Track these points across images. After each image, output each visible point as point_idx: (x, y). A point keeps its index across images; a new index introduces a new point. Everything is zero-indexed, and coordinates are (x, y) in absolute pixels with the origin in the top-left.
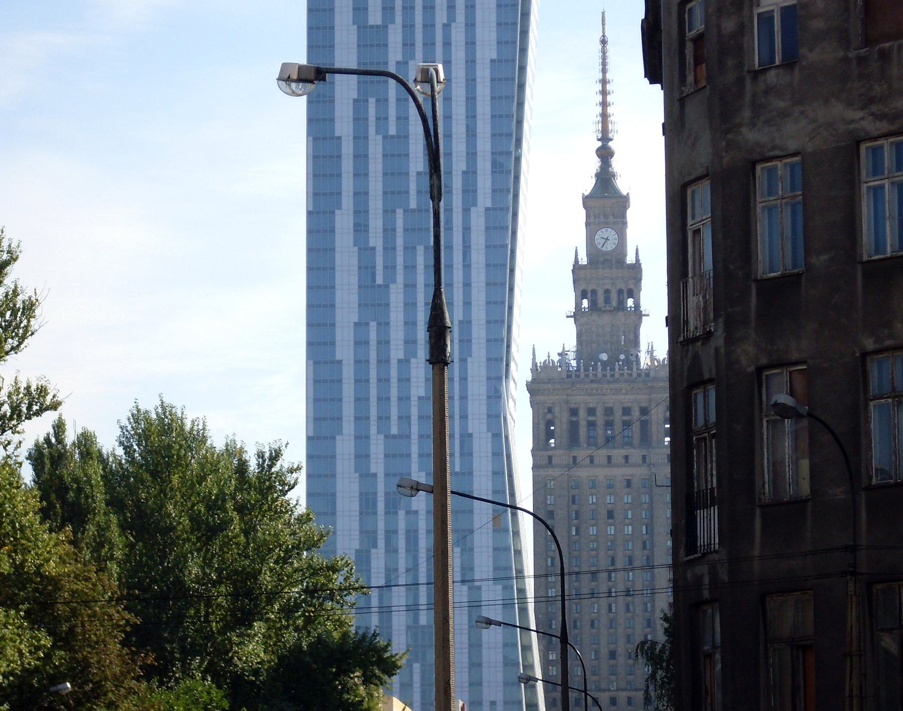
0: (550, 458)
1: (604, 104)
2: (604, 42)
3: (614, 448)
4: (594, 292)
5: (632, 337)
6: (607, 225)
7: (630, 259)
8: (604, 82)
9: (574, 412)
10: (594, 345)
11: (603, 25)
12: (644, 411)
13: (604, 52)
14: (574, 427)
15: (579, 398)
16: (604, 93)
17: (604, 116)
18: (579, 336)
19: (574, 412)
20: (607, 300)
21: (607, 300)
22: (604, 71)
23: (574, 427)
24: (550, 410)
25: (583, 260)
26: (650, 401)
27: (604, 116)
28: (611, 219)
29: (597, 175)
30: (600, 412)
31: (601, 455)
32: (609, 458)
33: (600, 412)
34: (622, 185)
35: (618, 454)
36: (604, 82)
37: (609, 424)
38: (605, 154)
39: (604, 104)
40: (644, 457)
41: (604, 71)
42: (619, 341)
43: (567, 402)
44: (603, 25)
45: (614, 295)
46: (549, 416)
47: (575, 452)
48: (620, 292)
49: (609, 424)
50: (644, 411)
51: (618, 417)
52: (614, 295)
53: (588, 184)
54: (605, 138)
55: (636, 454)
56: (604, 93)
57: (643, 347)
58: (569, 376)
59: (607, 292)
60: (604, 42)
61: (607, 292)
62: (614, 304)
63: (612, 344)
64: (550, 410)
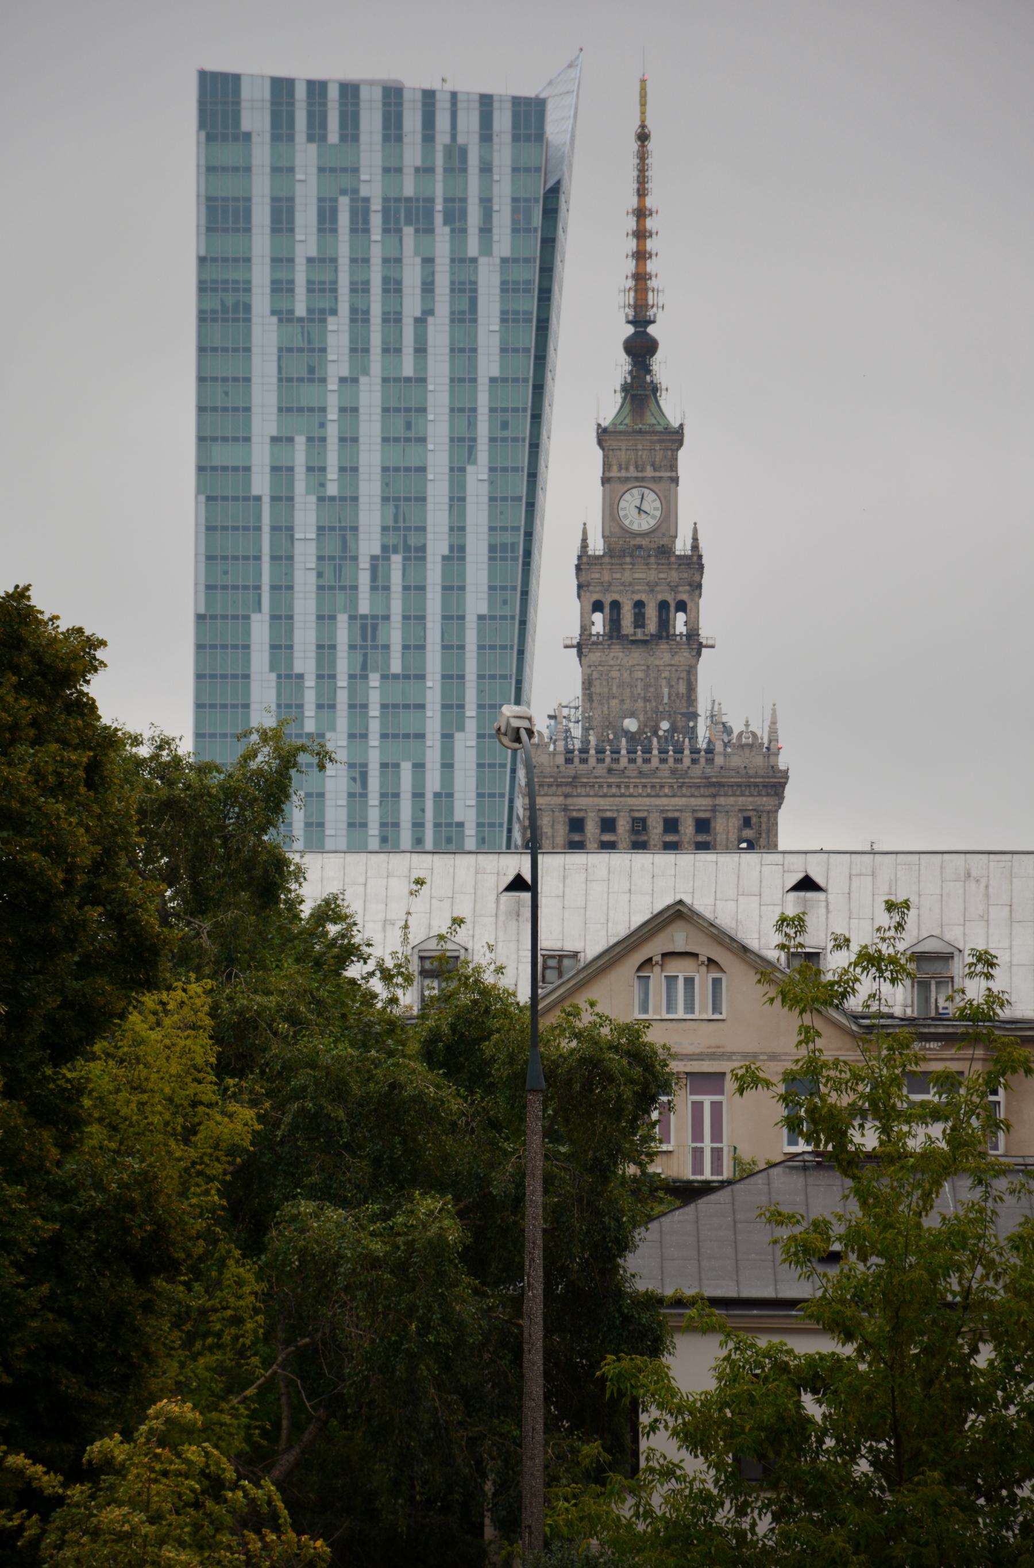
1: (641, 256)
4: (616, 605)
5: (682, 688)
7: (682, 546)
8: (641, 213)
10: (614, 703)
11: (643, 104)
13: (642, 157)
15: (583, 802)
16: (641, 234)
17: (641, 279)
18: (588, 684)
20: (639, 620)
21: (639, 620)
22: (642, 193)
25: (597, 546)
26: (714, 809)
27: (641, 279)
28: (649, 472)
29: (626, 388)
34: (672, 407)
36: (641, 213)
38: (641, 349)
39: (641, 256)
41: (642, 193)
42: (658, 697)
43: (565, 809)
44: (643, 104)
45: (651, 613)
48: (663, 606)
52: (651, 613)
53: (610, 407)
54: (641, 319)
56: (641, 234)
57: (703, 707)
58: (569, 761)
59: (639, 605)
61: (639, 605)
63: (646, 700)
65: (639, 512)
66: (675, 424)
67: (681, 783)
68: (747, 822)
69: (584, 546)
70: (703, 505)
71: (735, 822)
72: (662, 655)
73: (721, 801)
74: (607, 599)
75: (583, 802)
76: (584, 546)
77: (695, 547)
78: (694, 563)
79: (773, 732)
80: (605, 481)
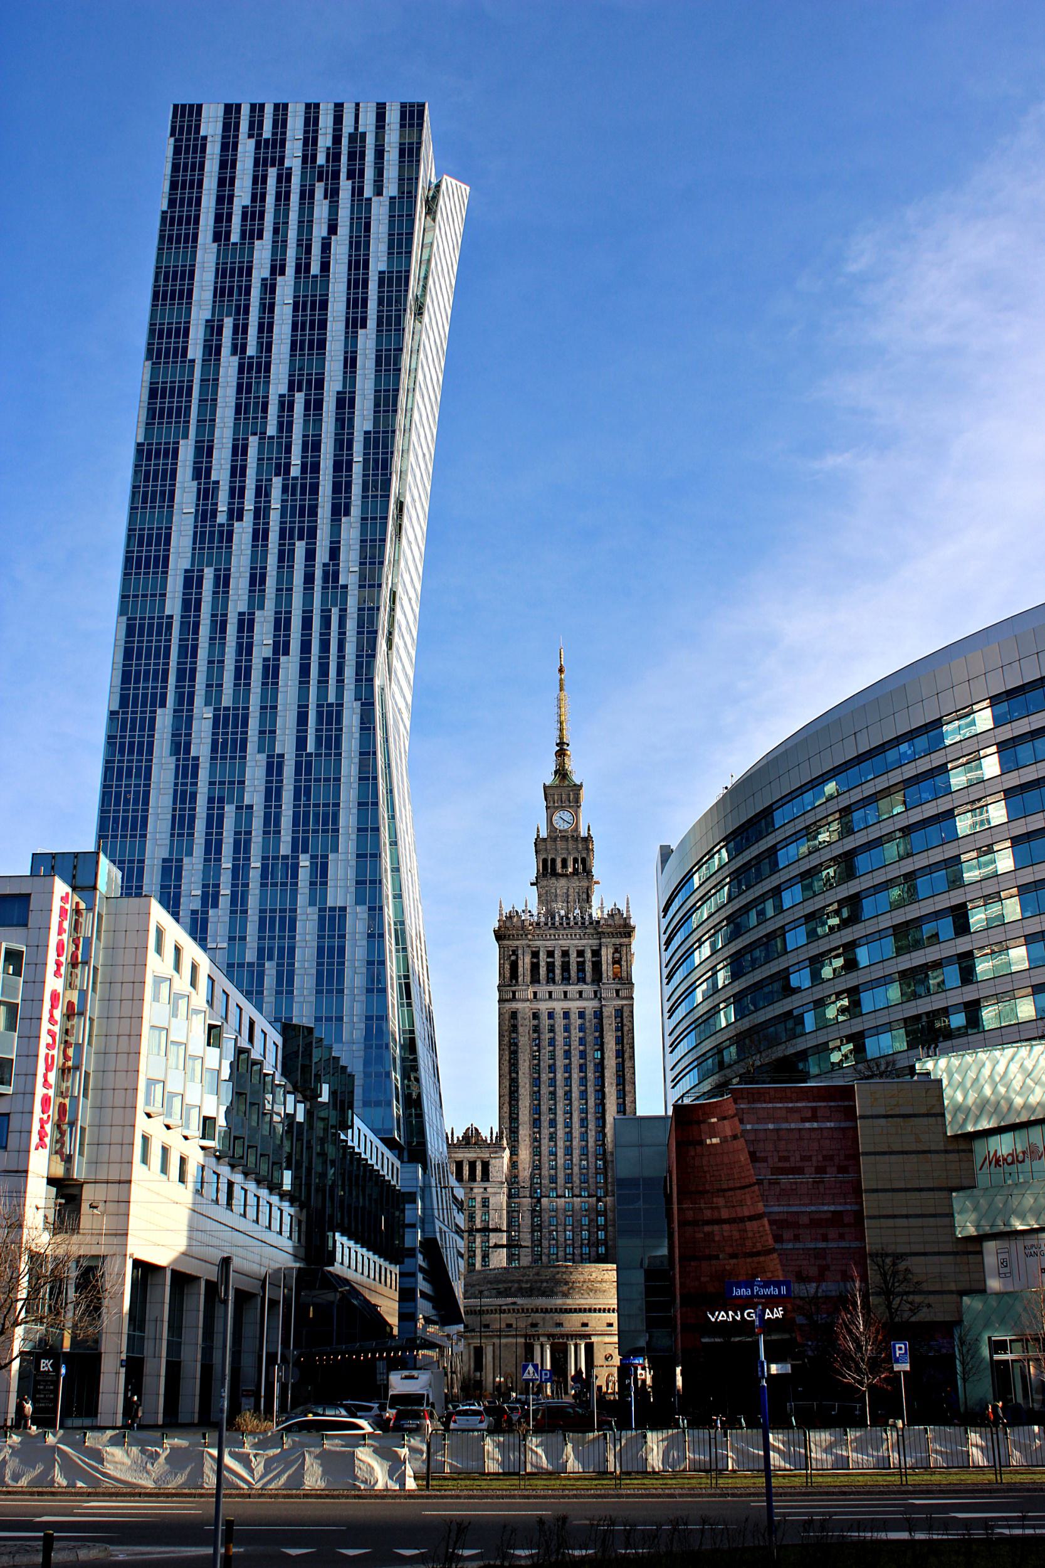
0: (514, 993)
2: (561, 671)
3: (570, 984)
4: (553, 861)
6: (563, 808)
7: (583, 833)
14: (535, 967)
15: (538, 943)
18: (540, 896)
23: (535, 967)
25: (544, 834)
31: (558, 990)
32: (565, 993)
35: (573, 989)
37: (566, 967)
38: (561, 753)
40: (595, 992)
45: (570, 863)
48: (575, 861)
49: (566, 967)
50: (596, 953)
51: (573, 958)
52: (570, 863)
53: (549, 779)
54: (561, 744)
55: (588, 989)
60: (561, 671)
64: (515, 952)
65: (562, 819)
66: (578, 783)
69: (538, 836)
70: (590, 818)
71: (611, 950)
73: (603, 940)
75: (538, 943)
76: (538, 836)
78: (588, 840)
79: (628, 911)
80: (547, 808)
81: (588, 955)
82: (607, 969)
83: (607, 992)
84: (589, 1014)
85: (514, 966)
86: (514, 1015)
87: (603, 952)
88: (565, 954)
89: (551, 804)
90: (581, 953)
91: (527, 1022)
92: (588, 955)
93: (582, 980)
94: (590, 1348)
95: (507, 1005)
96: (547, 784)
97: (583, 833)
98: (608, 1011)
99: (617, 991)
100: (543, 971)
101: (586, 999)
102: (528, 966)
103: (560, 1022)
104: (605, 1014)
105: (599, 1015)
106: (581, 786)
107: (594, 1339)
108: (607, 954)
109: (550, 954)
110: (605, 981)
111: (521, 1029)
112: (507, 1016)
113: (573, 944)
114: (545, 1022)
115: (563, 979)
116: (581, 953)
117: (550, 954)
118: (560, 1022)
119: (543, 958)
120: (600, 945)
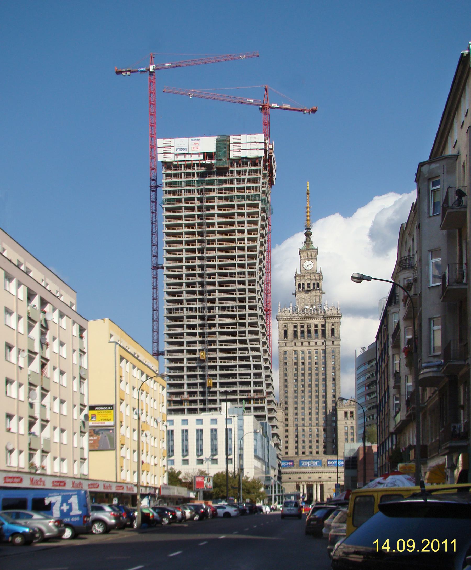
0: (286, 343)
4: (303, 284)
5: (318, 300)
6: (308, 259)
9: (295, 327)
12: (323, 326)
14: (295, 332)
19: (295, 327)
23: (295, 332)
24: (285, 326)
25: (299, 272)
28: (310, 258)
30: (306, 327)
32: (309, 343)
33: (306, 327)
37: (309, 332)
46: (285, 328)
47: (296, 341)
48: (314, 284)
49: (309, 332)
51: (313, 328)
53: (302, 246)
59: (309, 284)
61: (309, 284)
62: (312, 288)
65: (308, 265)
66: (316, 248)
67: (318, 318)
68: (333, 325)
72: (313, 293)
74: (302, 283)
77: (321, 272)
78: (320, 275)
81: (320, 327)
82: (328, 333)
83: (329, 343)
84: (320, 351)
85: (286, 332)
86: (286, 353)
87: (327, 325)
88: (309, 326)
89: (303, 258)
90: (316, 326)
91: (291, 356)
92: (320, 327)
93: (317, 337)
94: (322, 486)
95: (283, 349)
96: (301, 248)
97: (318, 272)
98: (329, 350)
99: (333, 342)
100: (299, 333)
101: (319, 346)
102: (292, 332)
103: (307, 355)
104: (327, 352)
105: (325, 352)
106: (317, 249)
107: (324, 483)
108: (328, 328)
109: (302, 326)
110: (327, 338)
111: (289, 359)
112: (283, 353)
113: (313, 322)
114: (300, 355)
115: (308, 336)
116: (316, 326)
117: (302, 326)
118: (307, 355)
119: (299, 329)
120: (325, 323)
